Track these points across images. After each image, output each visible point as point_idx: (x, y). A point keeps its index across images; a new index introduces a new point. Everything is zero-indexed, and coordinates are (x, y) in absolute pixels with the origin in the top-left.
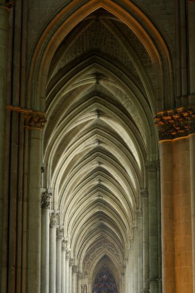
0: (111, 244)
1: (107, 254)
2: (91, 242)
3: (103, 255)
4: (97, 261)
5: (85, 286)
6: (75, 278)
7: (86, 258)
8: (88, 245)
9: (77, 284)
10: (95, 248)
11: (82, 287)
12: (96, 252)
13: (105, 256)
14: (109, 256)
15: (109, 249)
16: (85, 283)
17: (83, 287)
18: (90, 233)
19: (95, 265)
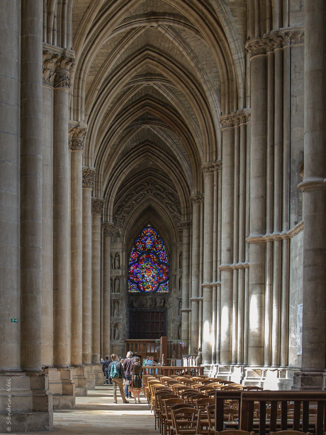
0: (159, 187)
1: (153, 204)
2: (127, 171)
3: (146, 205)
4: (137, 215)
5: (117, 255)
6: (98, 223)
7: (118, 210)
8: (123, 177)
9: (104, 251)
10: (132, 194)
11: (111, 256)
12: (135, 200)
13: (150, 210)
14: (157, 208)
15: (155, 195)
16: (117, 251)
17: (114, 256)
18: (125, 154)
19: (132, 221)
